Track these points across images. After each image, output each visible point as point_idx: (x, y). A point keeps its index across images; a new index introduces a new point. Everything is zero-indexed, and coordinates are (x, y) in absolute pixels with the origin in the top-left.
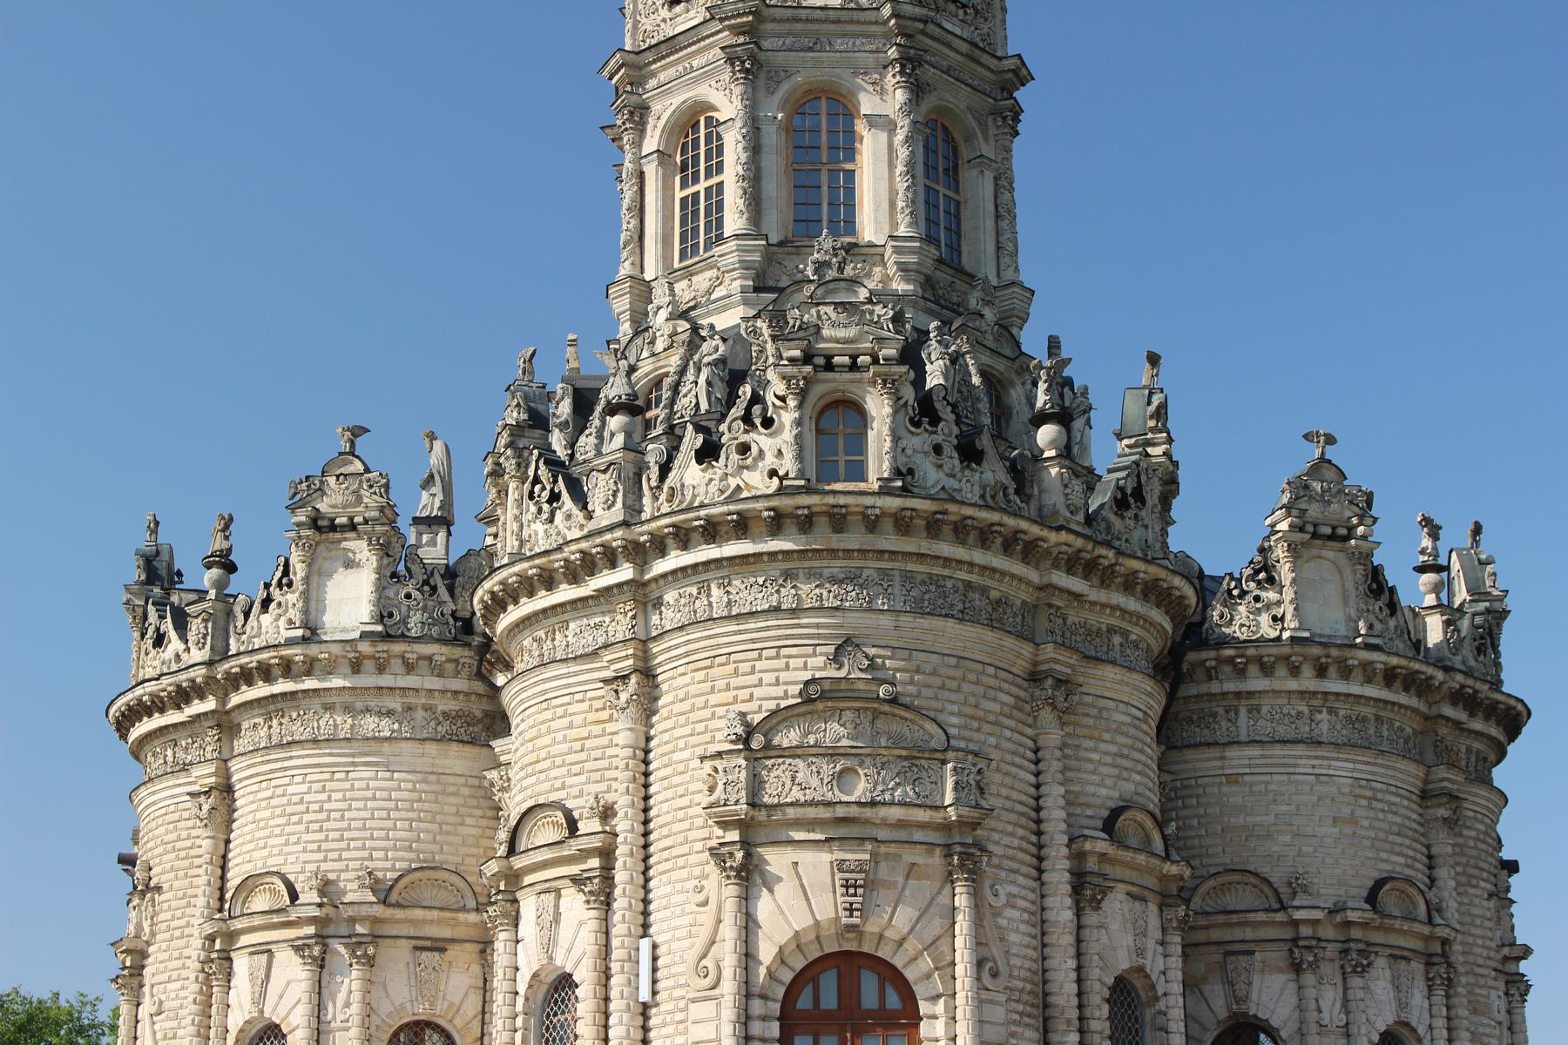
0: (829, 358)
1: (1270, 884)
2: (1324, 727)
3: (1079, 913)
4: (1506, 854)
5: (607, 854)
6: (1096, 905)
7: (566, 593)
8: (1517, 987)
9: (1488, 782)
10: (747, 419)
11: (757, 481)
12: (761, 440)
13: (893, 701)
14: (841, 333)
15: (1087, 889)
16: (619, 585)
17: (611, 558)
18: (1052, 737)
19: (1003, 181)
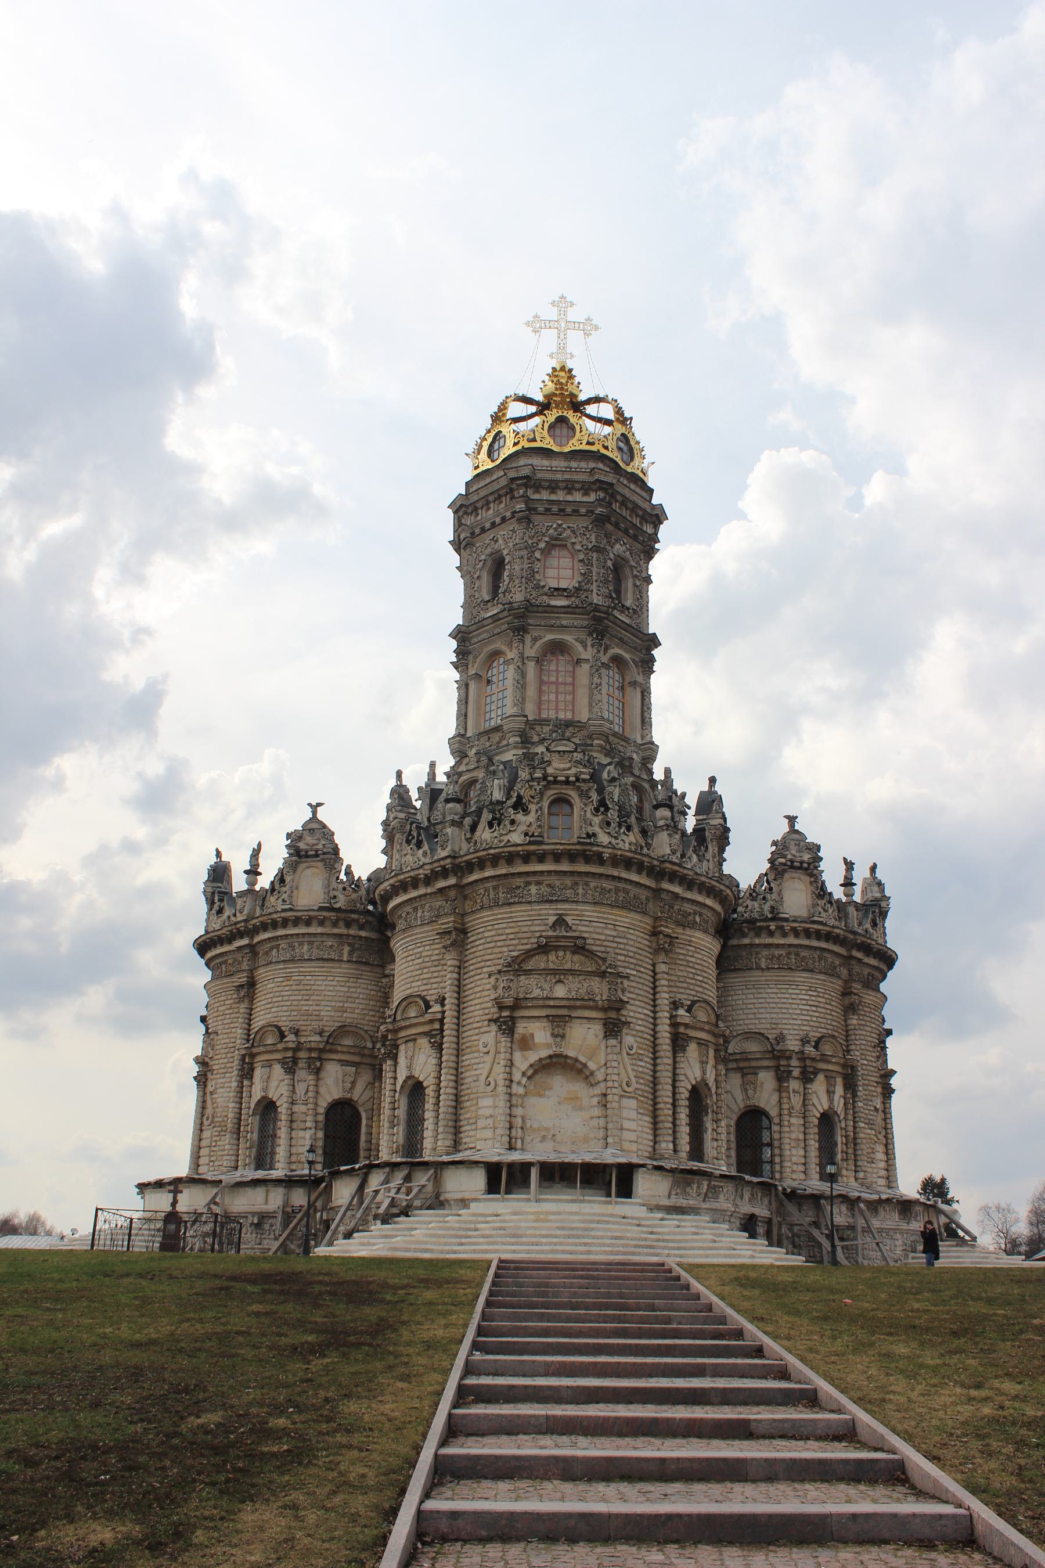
0: (555, 777)
1: (768, 1039)
3: (675, 1053)
4: (886, 1026)
5: (441, 1021)
6: (684, 1050)
7: (422, 891)
8: (888, 1092)
9: (878, 990)
11: (516, 837)
12: (520, 817)
13: (583, 948)
14: (562, 766)
15: (678, 1043)
16: (449, 887)
17: (445, 873)
18: (661, 968)
19: (645, 693)
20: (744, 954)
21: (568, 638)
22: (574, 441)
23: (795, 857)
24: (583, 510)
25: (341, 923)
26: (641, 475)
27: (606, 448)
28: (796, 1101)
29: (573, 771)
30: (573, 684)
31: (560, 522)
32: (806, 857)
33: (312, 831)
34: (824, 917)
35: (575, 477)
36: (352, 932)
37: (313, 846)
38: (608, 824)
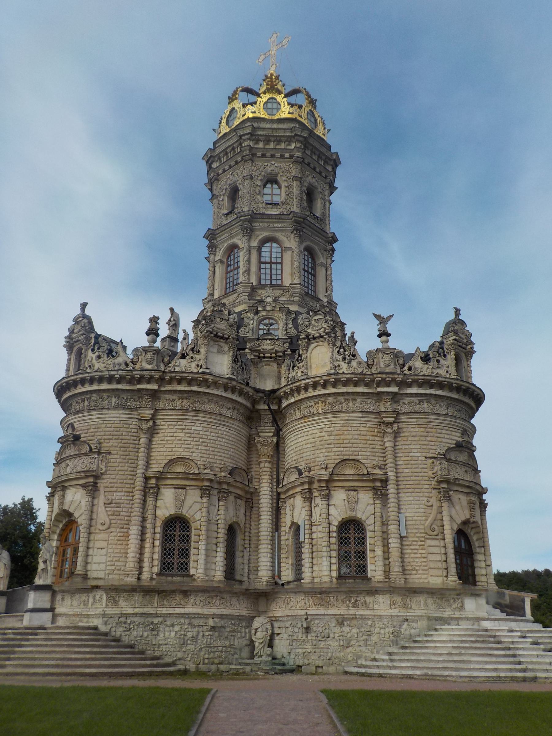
2: (320, 409)
35: (232, 142)
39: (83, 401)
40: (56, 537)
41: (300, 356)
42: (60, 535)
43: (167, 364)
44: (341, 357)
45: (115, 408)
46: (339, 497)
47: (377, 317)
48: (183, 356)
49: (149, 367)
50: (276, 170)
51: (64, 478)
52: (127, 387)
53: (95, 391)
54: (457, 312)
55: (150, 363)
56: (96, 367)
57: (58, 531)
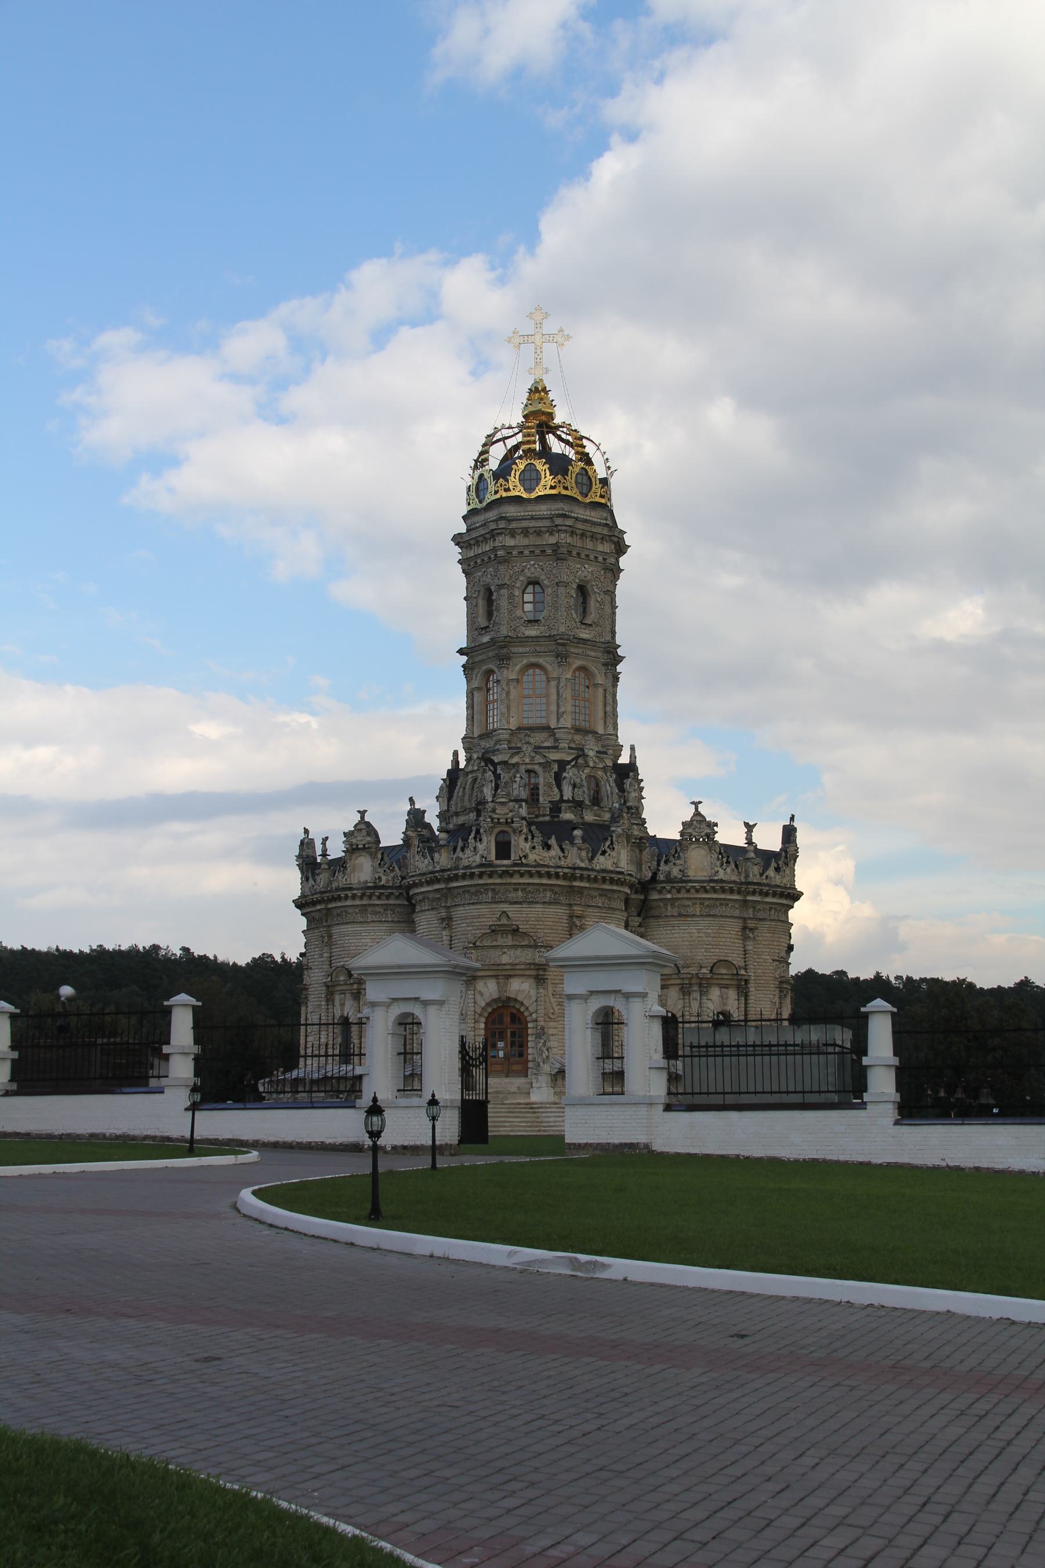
10: (475, 838)
20: (662, 904)
21: (541, 661)
22: (540, 486)
23: (699, 829)
24: (549, 551)
25: (384, 898)
26: (603, 501)
27: (566, 488)
28: (695, 1006)
29: (511, 814)
30: (547, 696)
31: (532, 563)
32: (708, 831)
33: (360, 830)
34: (721, 875)
35: (540, 524)
36: (391, 902)
37: (363, 837)
38: (534, 848)
39: (516, 890)
40: (484, 1020)
41: (676, 851)
42: (487, 1018)
43: (591, 860)
44: (718, 863)
45: (550, 903)
46: (715, 993)
47: (746, 825)
48: (604, 853)
49: (582, 865)
50: (589, 578)
51: (509, 967)
52: (564, 883)
53: (533, 884)
54: (792, 818)
55: (582, 861)
56: (532, 857)
57: (486, 1015)
